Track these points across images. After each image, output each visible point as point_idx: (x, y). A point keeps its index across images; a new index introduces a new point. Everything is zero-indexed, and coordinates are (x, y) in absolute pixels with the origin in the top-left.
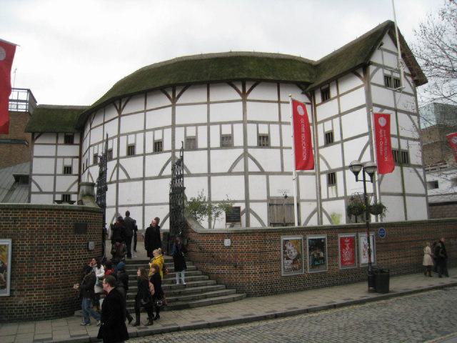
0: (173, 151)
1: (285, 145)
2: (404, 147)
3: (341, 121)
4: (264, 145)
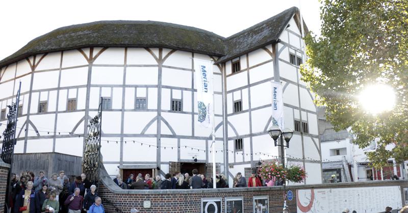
0: (87, 110)
1: (195, 112)
2: (304, 119)
3: (249, 91)
4: (176, 110)
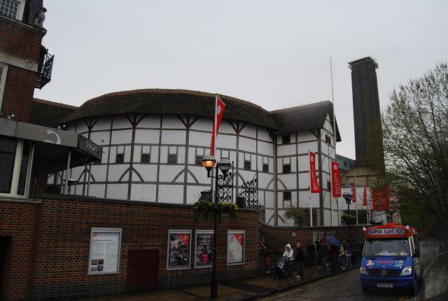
0: (186, 164)
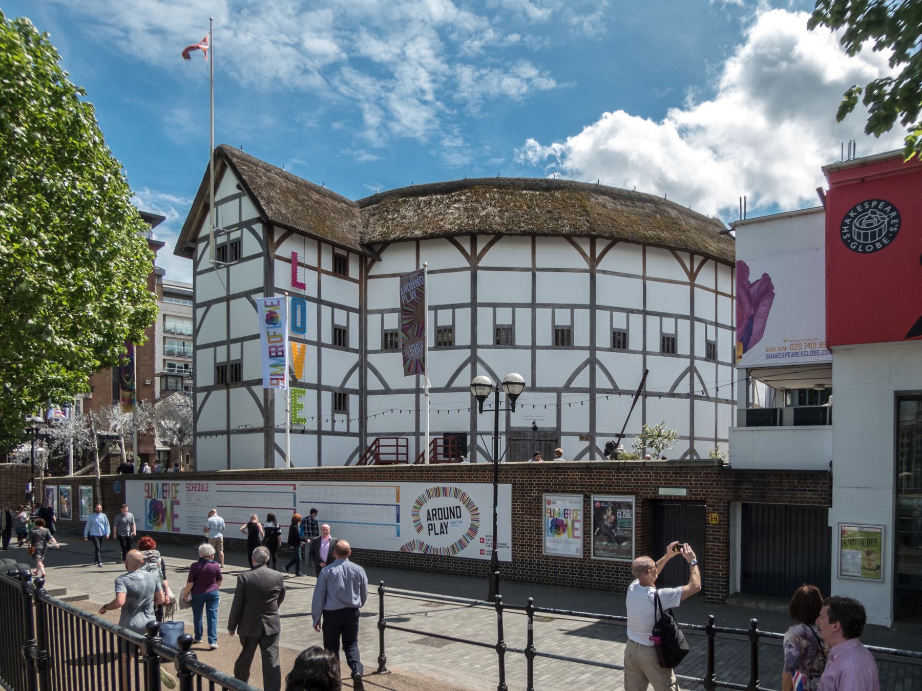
0: (474, 346)
4: (619, 347)
